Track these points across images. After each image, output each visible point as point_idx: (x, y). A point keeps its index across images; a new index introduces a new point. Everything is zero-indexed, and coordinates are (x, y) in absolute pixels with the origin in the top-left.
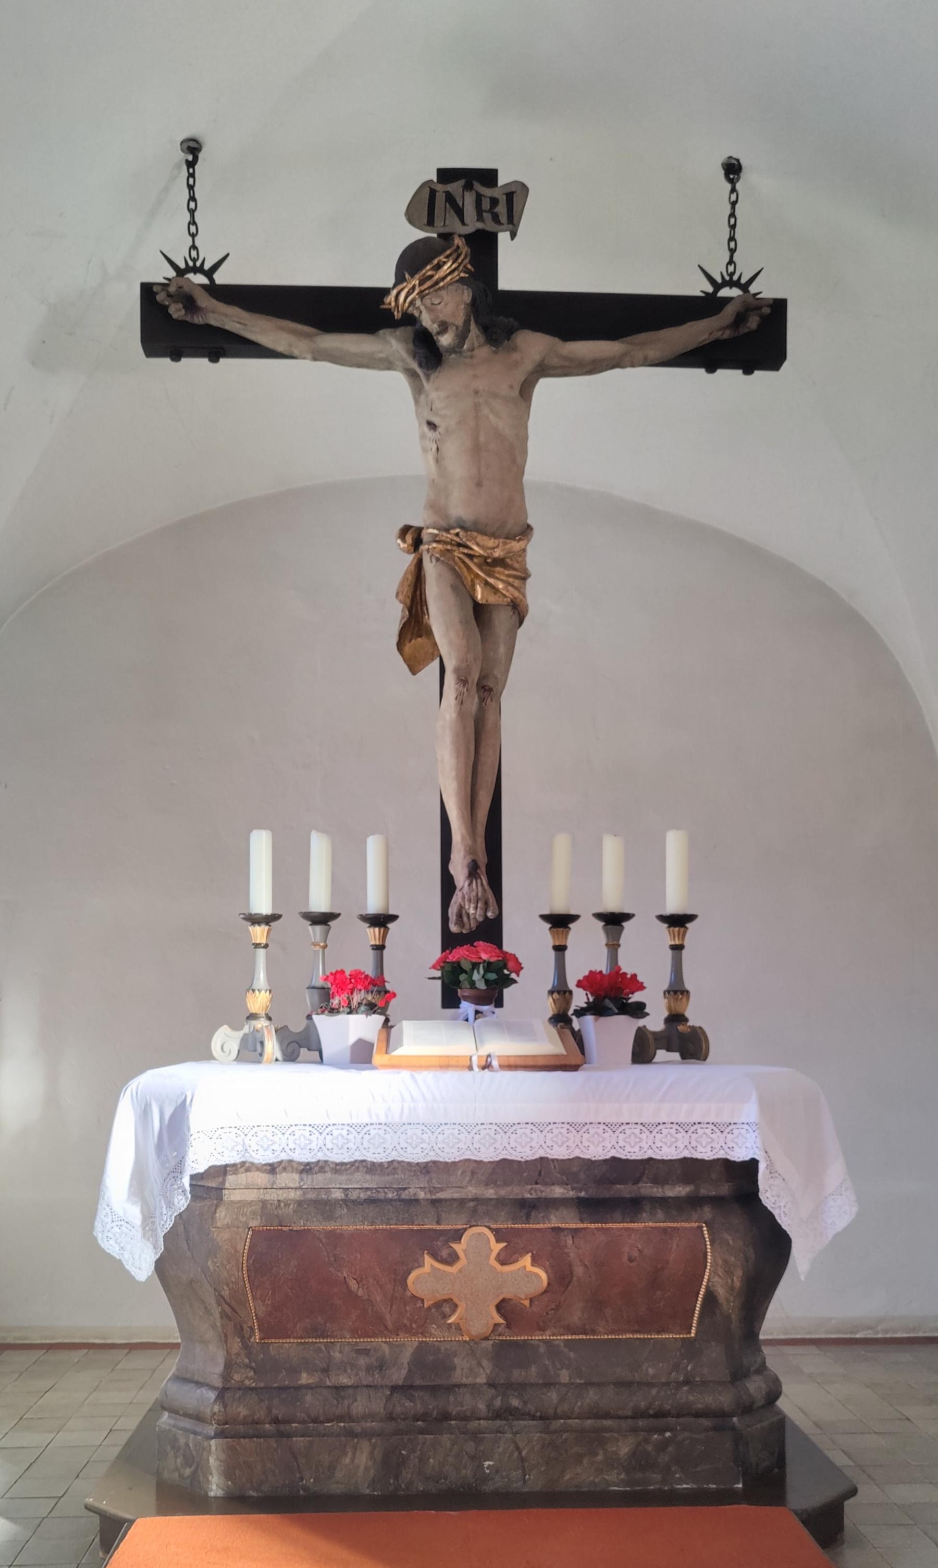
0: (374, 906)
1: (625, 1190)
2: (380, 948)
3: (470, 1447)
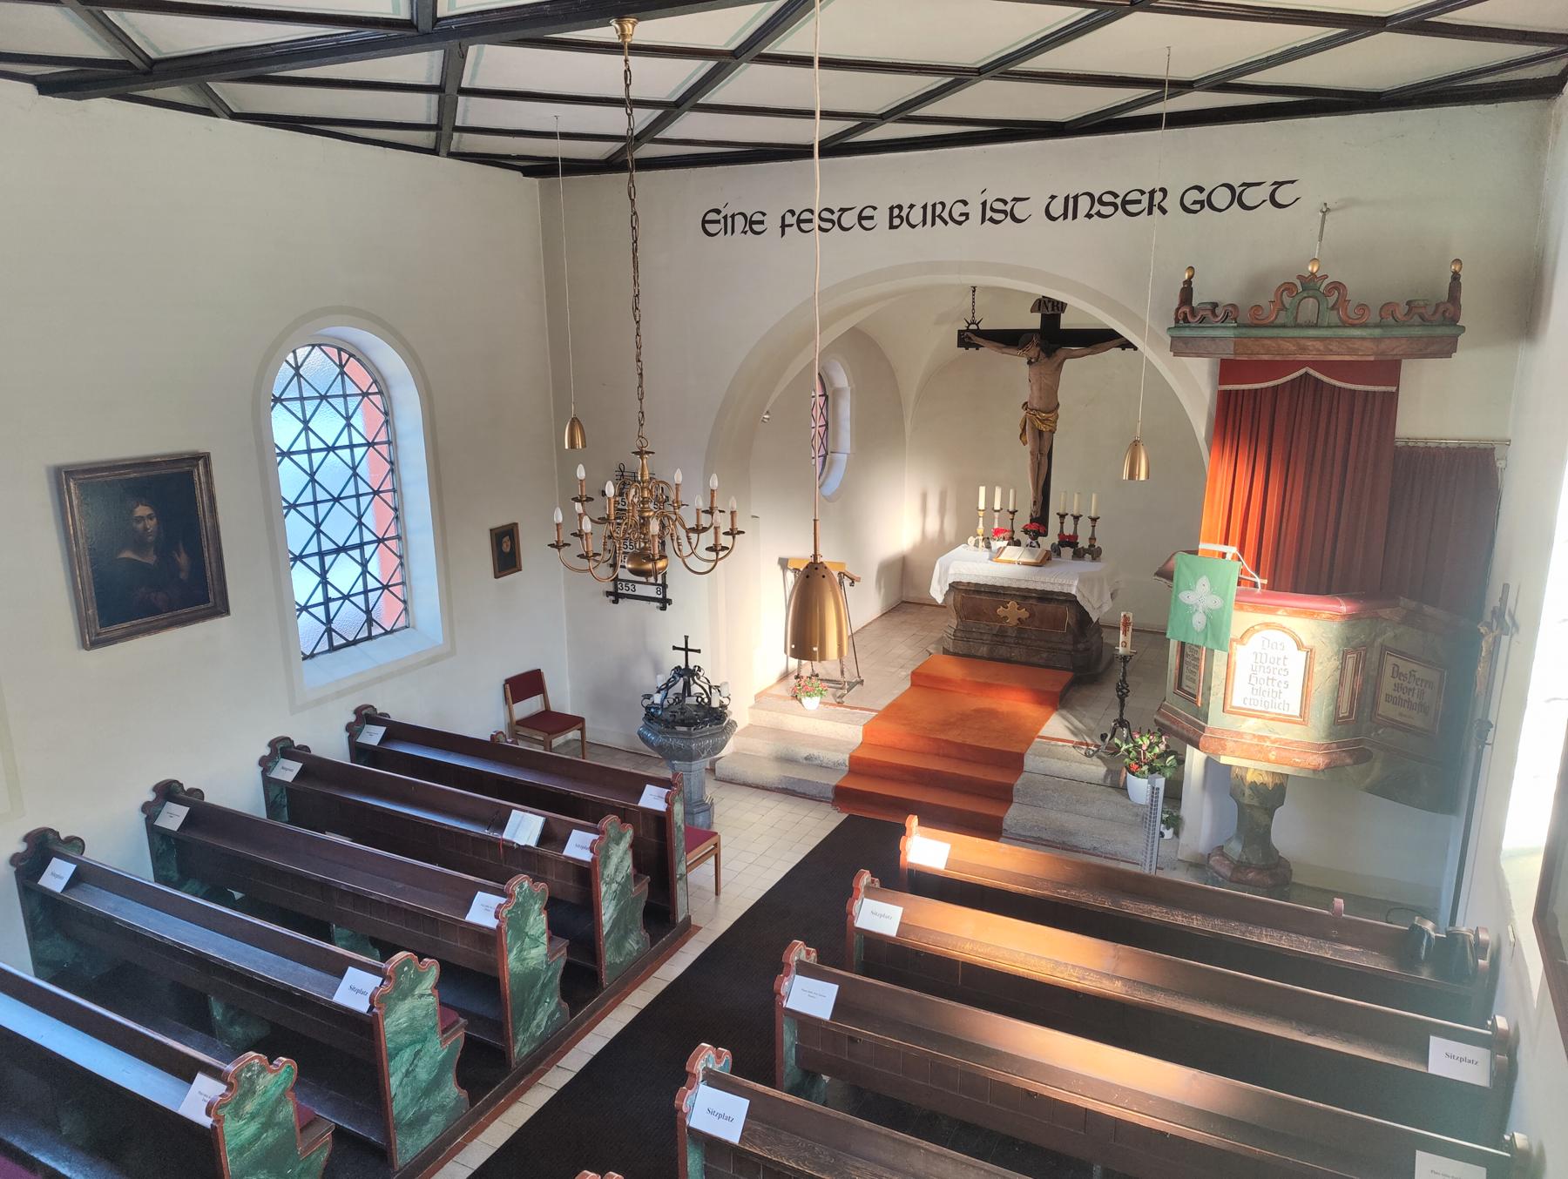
0: (1011, 509)
1: (1050, 597)
2: (1012, 519)
3: (1009, 650)
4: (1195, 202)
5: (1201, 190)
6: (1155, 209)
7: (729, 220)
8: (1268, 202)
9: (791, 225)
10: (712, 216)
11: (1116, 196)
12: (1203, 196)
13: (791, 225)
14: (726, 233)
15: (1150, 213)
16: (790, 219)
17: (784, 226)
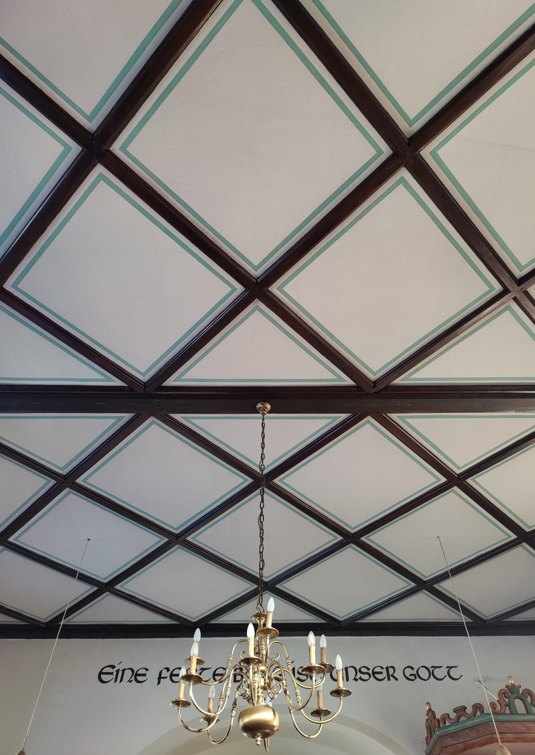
4: (411, 675)
5: (413, 669)
6: (390, 677)
7: (120, 673)
8: (448, 677)
9: (165, 678)
10: (109, 670)
11: (368, 669)
12: (414, 672)
13: (165, 678)
14: (116, 681)
15: (389, 679)
16: (165, 674)
17: (160, 678)
